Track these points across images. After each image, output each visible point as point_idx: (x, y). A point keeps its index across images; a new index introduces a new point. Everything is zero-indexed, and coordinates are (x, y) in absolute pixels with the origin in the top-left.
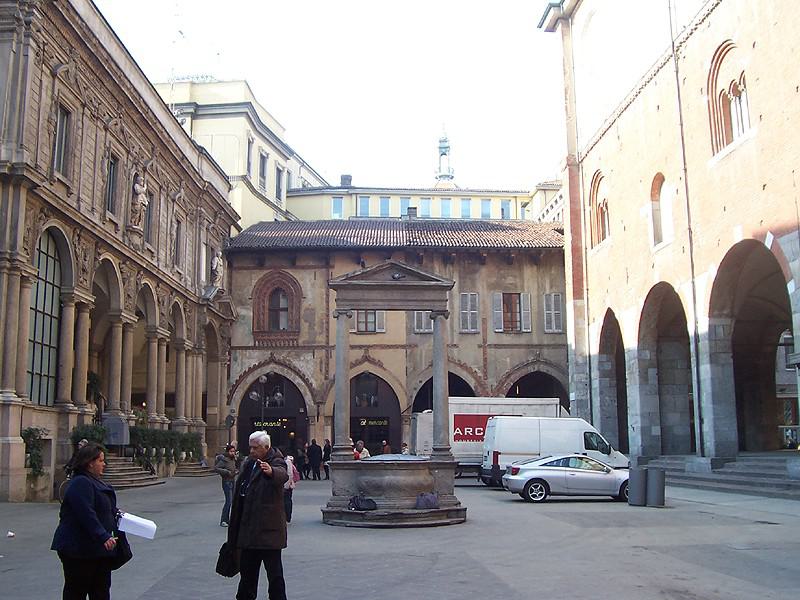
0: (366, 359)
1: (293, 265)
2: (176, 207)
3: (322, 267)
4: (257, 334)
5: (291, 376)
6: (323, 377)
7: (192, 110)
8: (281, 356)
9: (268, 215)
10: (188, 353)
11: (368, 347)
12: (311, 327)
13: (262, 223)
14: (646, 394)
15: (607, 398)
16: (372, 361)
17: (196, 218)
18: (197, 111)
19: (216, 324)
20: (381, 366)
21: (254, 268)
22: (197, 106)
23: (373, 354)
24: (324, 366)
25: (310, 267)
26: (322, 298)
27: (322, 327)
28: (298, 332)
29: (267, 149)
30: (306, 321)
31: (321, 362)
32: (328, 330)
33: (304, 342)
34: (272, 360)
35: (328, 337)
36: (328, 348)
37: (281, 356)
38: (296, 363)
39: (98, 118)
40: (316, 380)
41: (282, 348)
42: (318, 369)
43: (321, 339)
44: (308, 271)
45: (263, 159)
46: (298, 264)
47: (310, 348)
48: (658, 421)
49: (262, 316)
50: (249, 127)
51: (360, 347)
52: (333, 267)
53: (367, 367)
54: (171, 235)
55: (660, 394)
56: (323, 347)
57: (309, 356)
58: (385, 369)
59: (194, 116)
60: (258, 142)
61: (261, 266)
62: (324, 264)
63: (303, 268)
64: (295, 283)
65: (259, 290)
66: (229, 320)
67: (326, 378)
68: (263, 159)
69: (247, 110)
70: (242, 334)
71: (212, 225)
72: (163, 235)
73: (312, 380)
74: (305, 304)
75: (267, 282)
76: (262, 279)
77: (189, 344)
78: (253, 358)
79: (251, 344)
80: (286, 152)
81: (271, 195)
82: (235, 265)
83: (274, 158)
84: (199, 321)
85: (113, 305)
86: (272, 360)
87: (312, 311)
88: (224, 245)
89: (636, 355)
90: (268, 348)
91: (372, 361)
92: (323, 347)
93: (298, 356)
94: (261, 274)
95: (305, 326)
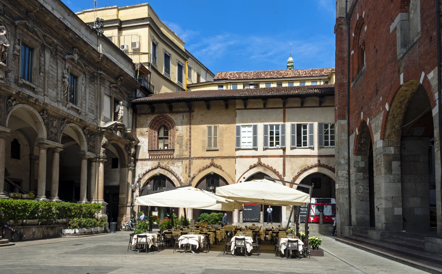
0: (212, 165)
1: (171, 111)
3: (187, 112)
5: (169, 175)
6: (187, 176)
8: (164, 164)
11: (213, 158)
12: (181, 147)
14: (390, 182)
15: (361, 187)
16: (217, 167)
20: (221, 169)
21: (149, 114)
23: (216, 162)
24: (188, 169)
26: (187, 130)
27: (187, 147)
30: (178, 143)
31: (186, 167)
32: (190, 148)
33: (176, 156)
34: (159, 166)
36: (190, 158)
37: (164, 164)
38: (172, 168)
40: (183, 178)
41: (164, 159)
42: (185, 171)
43: (186, 154)
44: (179, 114)
45: (167, 57)
47: (180, 159)
48: (401, 204)
49: (153, 142)
51: (208, 158)
52: (193, 111)
53: (212, 170)
55: (402, 181)
56: (187, 158)
57: (179, 164)
58: (223, 171)
67: (189, 176)
68: (167, 57)
71: (114, 85)
73: (181, 178)
74: (177, 134)
75: (157, 121)
76: (153, 120)
78: (149, 165)
83: (174, 57)
86: (159, 166)
87: (181, 137)
89: (382, 150)
90: (156, 159)
91: (217, 167)
92: (187, 158)
93: (173, 164)
94: (153, 117)
95: (177, 147)
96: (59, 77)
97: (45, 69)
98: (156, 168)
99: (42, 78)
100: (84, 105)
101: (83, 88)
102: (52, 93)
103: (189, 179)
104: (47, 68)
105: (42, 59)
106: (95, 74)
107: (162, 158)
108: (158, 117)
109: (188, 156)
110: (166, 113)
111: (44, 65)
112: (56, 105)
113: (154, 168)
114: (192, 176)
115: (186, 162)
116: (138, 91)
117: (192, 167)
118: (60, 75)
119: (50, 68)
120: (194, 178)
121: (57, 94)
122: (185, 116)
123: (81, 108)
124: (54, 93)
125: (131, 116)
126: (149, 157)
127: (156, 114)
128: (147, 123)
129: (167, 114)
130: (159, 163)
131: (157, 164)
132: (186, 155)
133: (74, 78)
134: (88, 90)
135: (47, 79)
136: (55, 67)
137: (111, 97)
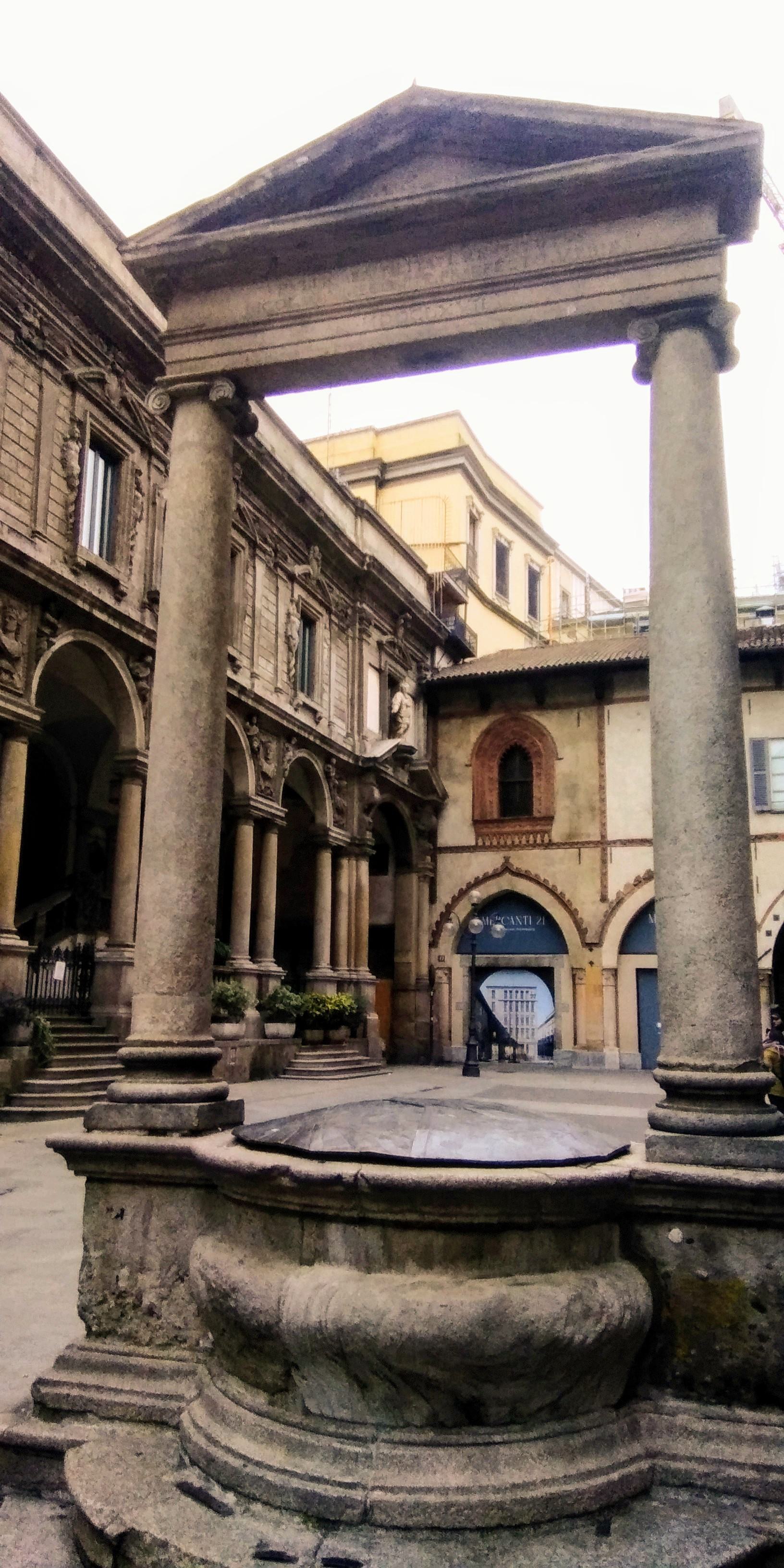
2: (298, 592)
4: (479, 823)
7: (375, 472)
9: (516, 641)
10: (338, 853)
13: (503, 651)
17: (349, 623)
18: (383, 476)
19: (405, 810)
21: (472, 714)
22: (384, 467)
25: (569, 706)
28: (549, 819)
29: (508, 533)
35: (604, 825)
36: (603, 844)
39: (43, 354)
46: (549, 701)
50: (468, 490)
54: (288, 638)
56: (596, 844)
59: (381, 483)
60: (489, 522)
61: (484, 709)
62: (593, 695)
63: (557, 707)
64: (542, 733)
65: (479, 751)
66: (430, 801)
67: (604, 899)
69: (461, 460)
70: (455, 825)
71: (389, 637)
72: (264, 639)
76: (487, 732)
77: (337, 835)
79: (473, 843)
80: (543, 545)
81: (517, 606)
82: (442, 711)
84: (361, 798)
85: (125, 743)
86: (506, 868)
88: (419, 680)
92: (596, 844)
96: (280, 625)
97: (254, 607)
98: (496, 875)
99: (248, 631)
100: (325, 697)
101: (326, 651)
102: (264, 667)
103: (604, 907)
104: (258, 605)
105: (250, 580)
106: (349, 611)
107: (539, 841)
108: (501, 722)
109: (598, 838)
110: (527, 709)
111: (254, 597)
112: (273, 699)
113: (490, 871)
114: (612, 896)
115: (591, 855)
116: (438, 654)
117: (611, 868)
118: (282, 619)
119: (264, 602)
120: (620, 902)
121: (276, 670)
122: (582, 715)
123: (321, 705)
124: (270, 668)
125: (422, 721)
126: (477, 840)
127: (495, 713)
128: (468, 741)
129: (527, 714)
130: (507, 859)
131: (502, 861)
132: (589, 835)
133: (308, 622)
134: (334, 656)
135: (256, 633)
136: (272, 598)
137: (379, 671)
